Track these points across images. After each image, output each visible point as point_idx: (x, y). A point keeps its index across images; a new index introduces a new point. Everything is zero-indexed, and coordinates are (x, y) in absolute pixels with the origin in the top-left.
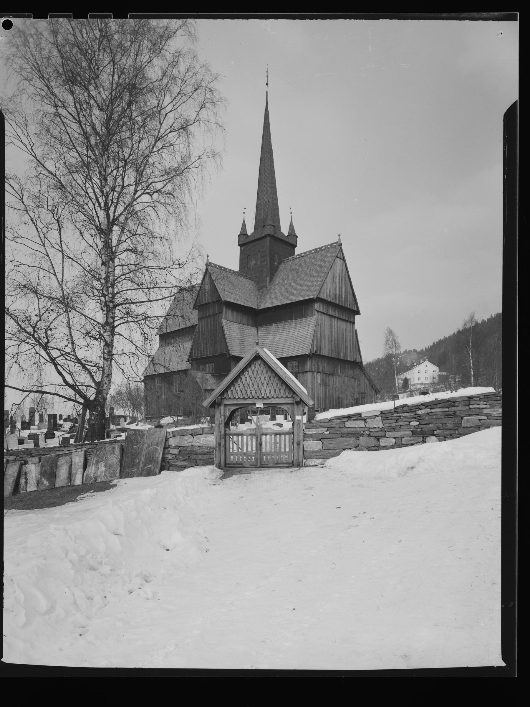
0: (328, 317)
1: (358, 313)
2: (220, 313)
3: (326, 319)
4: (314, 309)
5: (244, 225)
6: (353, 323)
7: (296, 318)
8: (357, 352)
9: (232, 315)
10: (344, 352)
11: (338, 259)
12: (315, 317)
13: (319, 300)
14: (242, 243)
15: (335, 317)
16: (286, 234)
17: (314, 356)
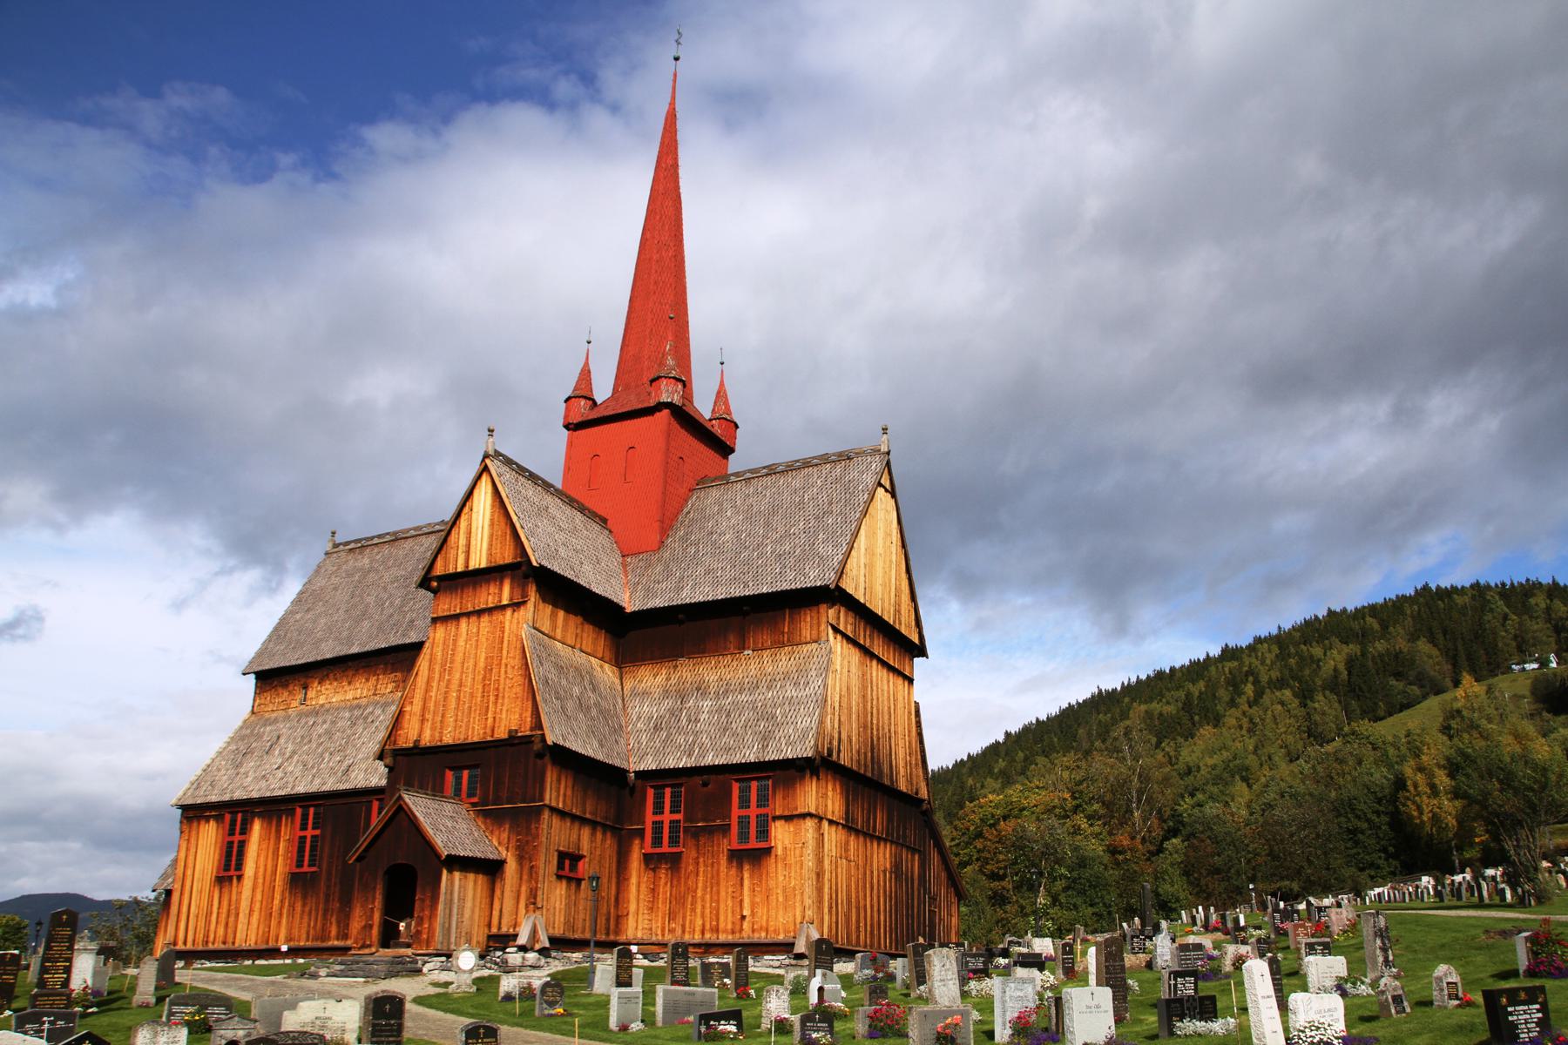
1: (920, 650)
2: (516, 605)
3: (855, 656)
4: (824, 619)
5: (585, 375)
6: (911, 681)
9: (553, 616)
11: (880, 491)
13: (834, 595)
14: (575, 419)
16: (707, 416)
17: (819, 765)
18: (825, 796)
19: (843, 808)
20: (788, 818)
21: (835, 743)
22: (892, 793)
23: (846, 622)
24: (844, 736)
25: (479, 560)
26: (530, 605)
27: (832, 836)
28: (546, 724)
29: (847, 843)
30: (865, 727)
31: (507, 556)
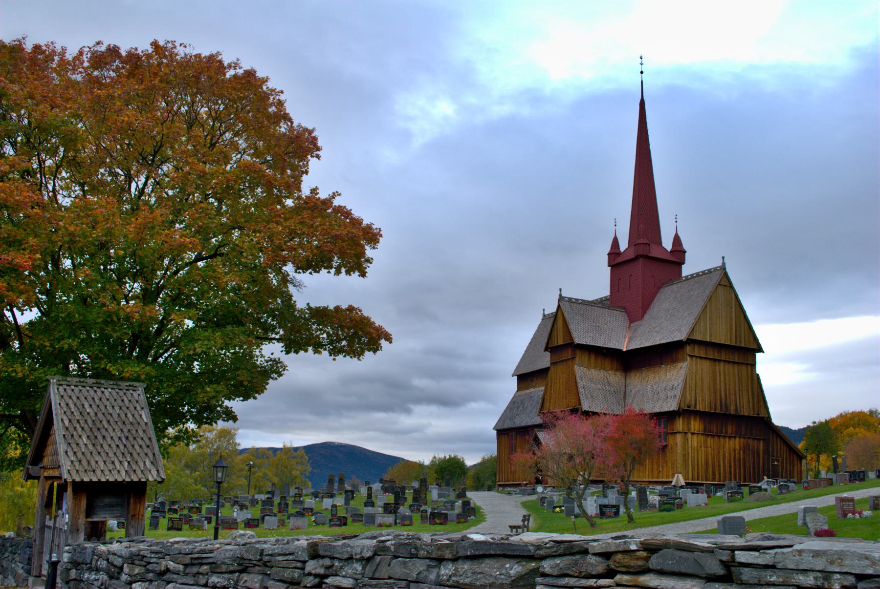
0: (708, 361)
1: (760, 350)
2: (573, 358)
3: (706, 365)
6: (753, 365)
7: (667, 364)
8: (762, 404)
9: (589, 358)
10: (736, 405)
12: (686, 364)
15: (719, 361)
17: (685, 412)
18: (689, 424)
19: (702, 427)
20: (672, 433)
21: (693, 402)
22: (738, 419)
23: (698, 351)
24: (699, 399)
25: (561, 342)
26: (577, 359)
27: (694, 441)
28: (582, 402)
29: (705, 442)
30: (715, 392)
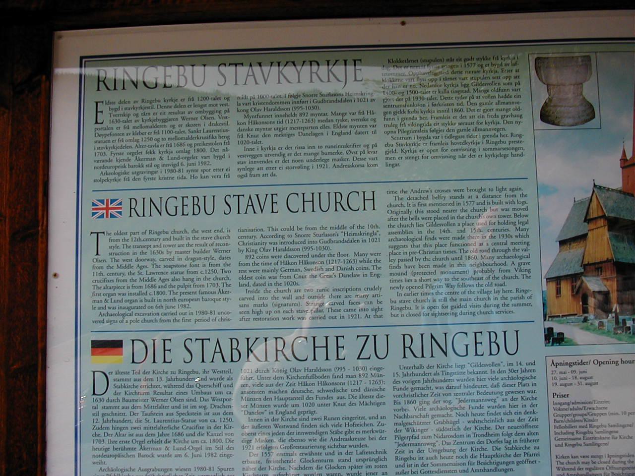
2: (605, 226)
5: (624, 152)
31: (601, 214)
